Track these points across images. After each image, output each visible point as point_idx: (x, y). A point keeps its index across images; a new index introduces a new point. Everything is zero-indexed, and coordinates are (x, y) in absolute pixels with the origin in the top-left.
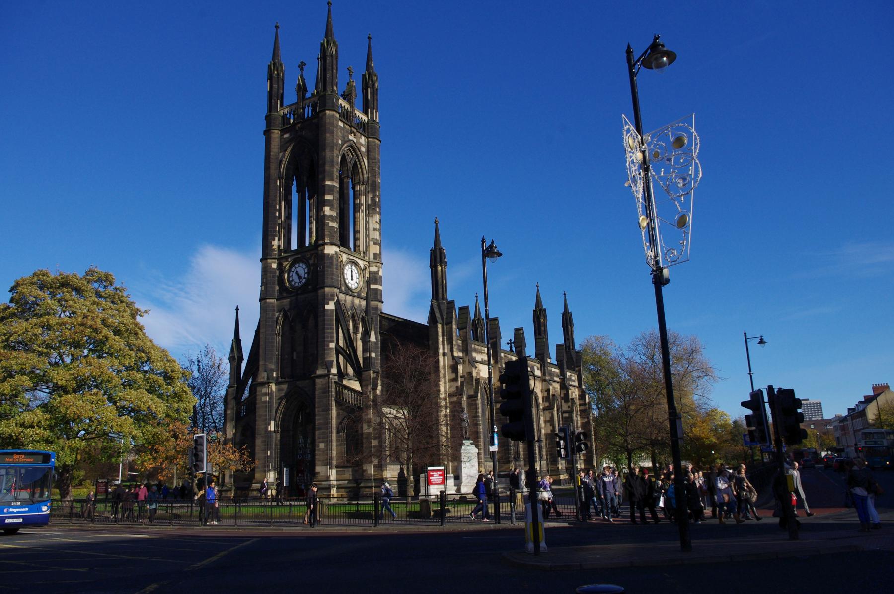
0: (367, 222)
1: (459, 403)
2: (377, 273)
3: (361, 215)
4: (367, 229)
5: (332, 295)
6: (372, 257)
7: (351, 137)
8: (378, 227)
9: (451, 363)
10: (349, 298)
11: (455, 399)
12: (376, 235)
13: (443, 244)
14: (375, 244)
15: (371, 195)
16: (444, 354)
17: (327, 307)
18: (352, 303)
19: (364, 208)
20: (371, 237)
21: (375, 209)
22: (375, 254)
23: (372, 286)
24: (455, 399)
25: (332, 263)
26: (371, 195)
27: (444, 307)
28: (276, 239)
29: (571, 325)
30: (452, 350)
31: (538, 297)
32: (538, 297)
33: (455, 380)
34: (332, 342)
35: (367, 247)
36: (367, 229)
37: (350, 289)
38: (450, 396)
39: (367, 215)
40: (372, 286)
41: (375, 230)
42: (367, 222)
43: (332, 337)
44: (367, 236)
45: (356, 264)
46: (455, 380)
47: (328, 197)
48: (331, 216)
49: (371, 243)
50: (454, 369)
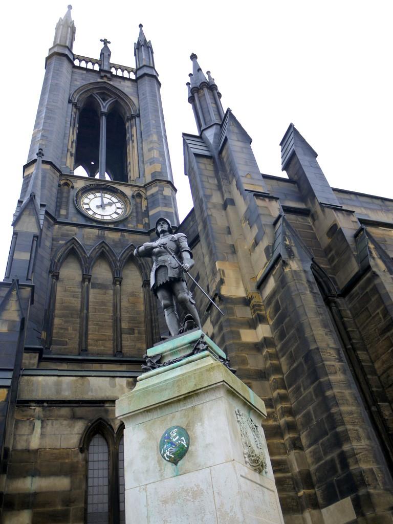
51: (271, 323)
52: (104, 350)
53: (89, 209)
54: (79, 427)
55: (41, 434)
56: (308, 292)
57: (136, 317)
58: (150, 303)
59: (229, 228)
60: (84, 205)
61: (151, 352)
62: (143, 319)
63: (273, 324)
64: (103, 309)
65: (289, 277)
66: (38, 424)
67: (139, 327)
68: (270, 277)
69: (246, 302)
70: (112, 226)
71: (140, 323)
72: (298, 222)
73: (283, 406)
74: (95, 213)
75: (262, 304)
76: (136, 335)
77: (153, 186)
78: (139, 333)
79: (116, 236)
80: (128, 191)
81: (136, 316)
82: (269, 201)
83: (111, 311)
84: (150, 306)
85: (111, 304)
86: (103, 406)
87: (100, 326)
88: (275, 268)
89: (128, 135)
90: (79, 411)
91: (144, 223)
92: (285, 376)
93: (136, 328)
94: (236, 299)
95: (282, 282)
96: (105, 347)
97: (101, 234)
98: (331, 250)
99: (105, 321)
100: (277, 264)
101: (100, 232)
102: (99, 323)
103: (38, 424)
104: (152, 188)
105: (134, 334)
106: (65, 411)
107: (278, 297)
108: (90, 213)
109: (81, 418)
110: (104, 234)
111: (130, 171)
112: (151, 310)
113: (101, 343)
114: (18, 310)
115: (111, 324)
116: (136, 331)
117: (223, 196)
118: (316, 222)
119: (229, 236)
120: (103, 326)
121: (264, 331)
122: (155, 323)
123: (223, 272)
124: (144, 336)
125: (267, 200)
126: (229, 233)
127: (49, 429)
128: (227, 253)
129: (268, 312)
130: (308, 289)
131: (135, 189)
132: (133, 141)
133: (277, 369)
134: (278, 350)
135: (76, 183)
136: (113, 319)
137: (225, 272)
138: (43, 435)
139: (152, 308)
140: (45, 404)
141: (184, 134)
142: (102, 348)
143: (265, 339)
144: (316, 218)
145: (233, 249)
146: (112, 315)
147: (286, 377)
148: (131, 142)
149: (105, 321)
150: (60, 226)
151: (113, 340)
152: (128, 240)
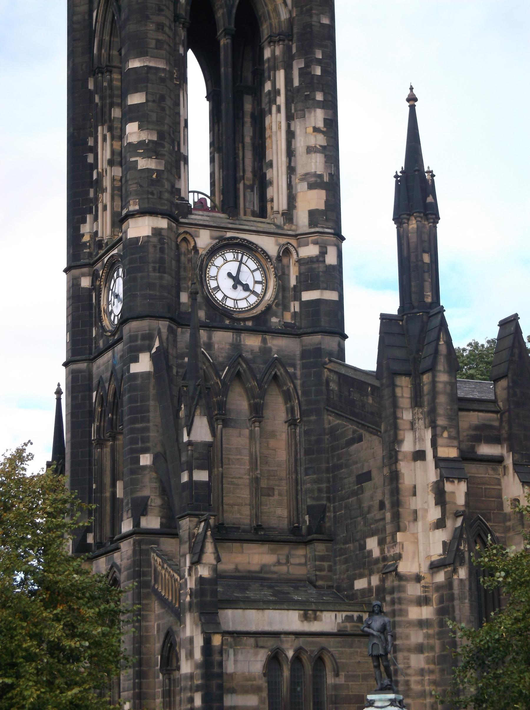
0: (290, 135)
4: (290, 153)
8: (321, 140)
10: (222, 339)
11: (440, 577)
12: (316, 164)
13: (429, 162)
14: (311, 187)
15: (298, 65)
18: (236, 347)
19: (281, 100)
20: (300, 171)
21: (310, 98)
23: (308, 296)
26: (298, 65)
28: (89, 218)
34: (145, 451)
35: (292, 199)
37: (226, 313)
38: (435, 567)
39: (290, 118)
40: (308, 296)
41: (310, 150)
42: (290, 135)
43: (145, 440)
44: (291, 170)
45: (250, 249)
46: (440, 524)
47: (136, 99)
48: (141, 143)
49: (301, 187)
50: (441, 497)
51: (435, 607)
52: (240, 518)
53: (218, 288)
54: (262, 656)
55: (235, 661)
56: (467, 601)
57: (276, 471)
58: (296, 455)
59: (415, 487)
60: (211, 282)
61: (370, 697)
62: (283, 474)
63: (436, 608)
64: (238, 459)
65: (456, 584)
66: (231, 652)
67: (279, 486)
68: (441, 570)
69: (418, 578)
70: (249, 324)
71: (281, 479)
72: (487, 475)
73: (430, 678)
74: (226, 297)
75: (431, 585)
76: (276, 497)
77: (310, 239)
78: (280, 494)
79: (252, 342)
80: (270, 245)
81: (276, 468)
82: (459, 482)
83: (247, 462)
84: (296, 460)
85: (246, 452)
86: (279, 637)
87: (234, 484)
88: (447, 568)
89: (268, 87)
90: (262, 641)
91: (292, 310)
92: (436, 655)
93: (276, 488)
94: (410, 575)
95: (449, 584)
96: (241, 514)
97: (237, 339)
98: (510, 520)
99: (240, 478)
100: (449, 567)
101: (235, 336)
102: (234, 480)
103: (231, 652)
104: (307, 245)
105: (274, 495)
106: (252, 641)
107: (445, 593)
108: (219, 296)
109: (263, 647)
110: (240, 340)
111: (271, 183)
112: (296, 466)
113: (236, 509)
114: (214, 553)
115: (248, 481)
116: (276, 493)
117: (415, 443)
118: (506, 477)
119: (414, 498)
120: (238, 485)
121: (426, 612)
122: (301, 486)
123: (403, 545)
124: (286, 498)
125: (456, 482)
126: (415, 494)
127: (240, 657)
128: (409, 522)
129: (435, 597)
130: (468, 598)
131: (283, 240)
132: (279, 110)
133: (432, 648)
134: (436, 631)
135: (198, 237)
136: (249, 475)
137: (405, 546)
138: (236, 661)
139: (299, 463)
140: (235, 635)
142: (238, 516)
143: (427, 620)
144: (507, 474)
145: (415, 515)
146: (248, 468)
147: (438, 656)
148: (274, 108)
149: (240, 478)
150: (183, 329)
151: (250, 505)
152: (270, 349)
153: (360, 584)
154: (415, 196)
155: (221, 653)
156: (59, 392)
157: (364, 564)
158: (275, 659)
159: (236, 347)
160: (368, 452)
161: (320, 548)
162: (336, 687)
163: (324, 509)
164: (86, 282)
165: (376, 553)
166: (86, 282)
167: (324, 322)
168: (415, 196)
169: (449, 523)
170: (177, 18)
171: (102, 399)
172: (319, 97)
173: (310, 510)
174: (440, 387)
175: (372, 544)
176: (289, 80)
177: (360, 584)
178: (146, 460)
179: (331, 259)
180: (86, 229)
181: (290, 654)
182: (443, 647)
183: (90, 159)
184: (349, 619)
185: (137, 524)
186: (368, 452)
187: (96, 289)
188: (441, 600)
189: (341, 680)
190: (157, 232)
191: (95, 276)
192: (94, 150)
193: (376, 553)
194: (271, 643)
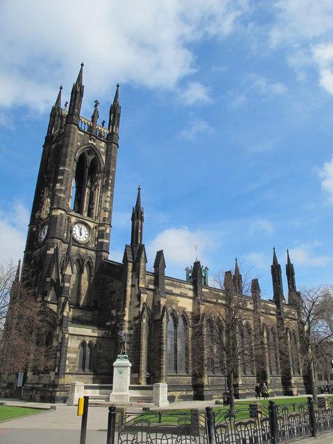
0: (101, 197)
1: (140, 324)
2: (104, 231)
3: (97, 193)
4: (100, 202)
5: (54, 243)
6: (102, 219)
7: (90, 142)
9: (137, 292)
11: (137, 322)
16: (133, 286)
17: (48, 252)
21: (107, 188)
22: (104, 218)
23: (100, 240)
24: (137, 322)
25: (56, 221)
26: (105, 179)
27: (136, 250)
29: (293, 274)
30: (138, 283)
31: (275, 256)
32: (275, 256)
33: (139, 306)
34: (49, 277)
35: (99, 214)
36: (100, 202)
40: (100, 240)
42: (101, 197)
45: (86, 225)
54: (79, 342)
79: (83, 251)
90: (79, 337)
129: (134, 327)
141: (126, 245)
153: (108, 323)
154: (137, 215)
155: (68, 340)
156: (20, 262)
157: (111, 318)
158: (83, 344)
159: (78, 251)
160: (116, 284)
161: (96, 312)
162: (100, 353)
163: (98, 301)
164: (34, 229)
165: (115, 314)
166: (34, 229)
167: (104, 249)
168: (137, 215)
169: (141, 306)
170: (75, 160)
171: (34, 262)
172: (110, 188)
173: (94, 302)
174: (141, 267)
175: (114, 312)
176: (102, 183)
177: (108, 323)
178: (48, 280)
179: (108, 231)
180: (37, 214)
181: (87, 342)
182: (136, 342)
183: (41, 196)
184: (105, 333)
185: (43, 298)
186: (116, 284)
187: (38, 231)
188: (137, 328)
189: (101, 351)
190: (61, 214)
191: (38, 228)
192: (43, 193)
193: (115, 314)
194: (82, 338)
